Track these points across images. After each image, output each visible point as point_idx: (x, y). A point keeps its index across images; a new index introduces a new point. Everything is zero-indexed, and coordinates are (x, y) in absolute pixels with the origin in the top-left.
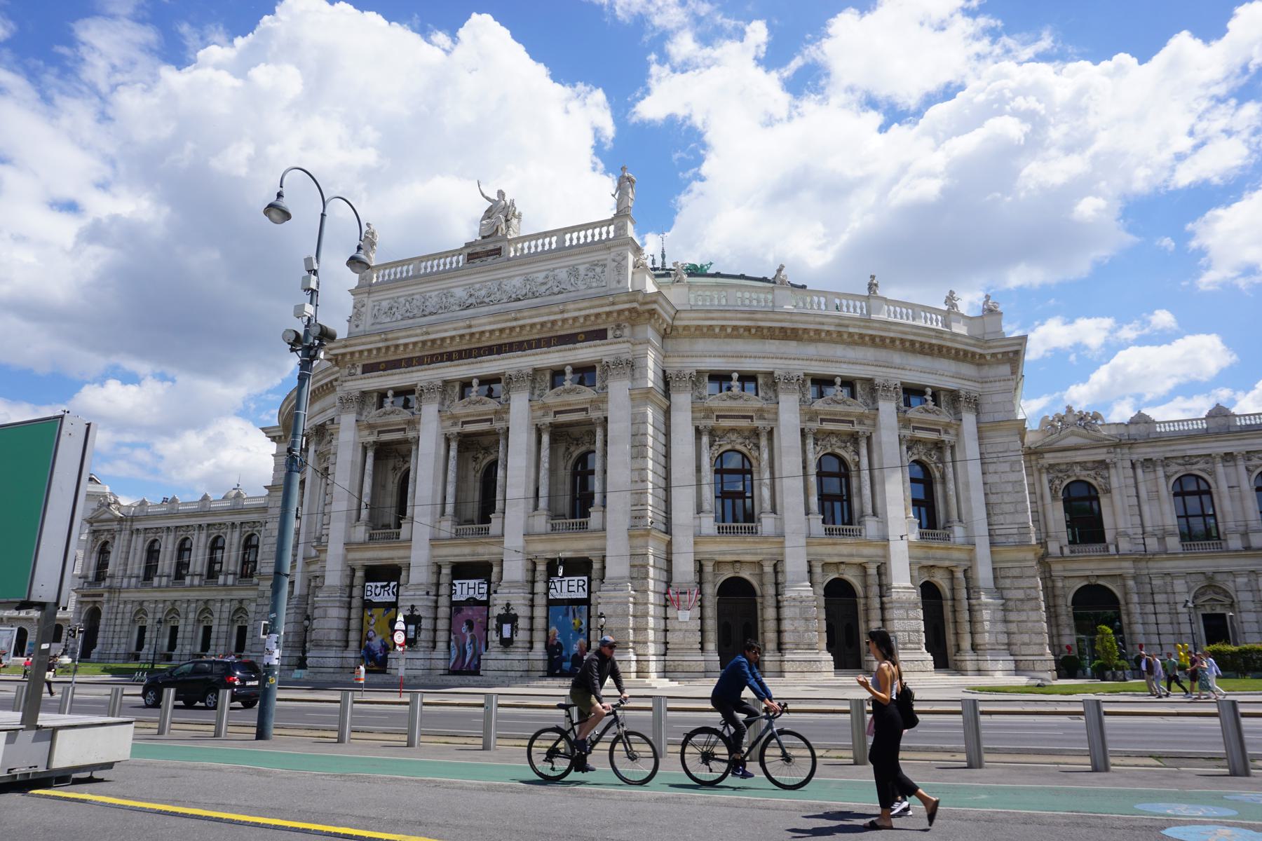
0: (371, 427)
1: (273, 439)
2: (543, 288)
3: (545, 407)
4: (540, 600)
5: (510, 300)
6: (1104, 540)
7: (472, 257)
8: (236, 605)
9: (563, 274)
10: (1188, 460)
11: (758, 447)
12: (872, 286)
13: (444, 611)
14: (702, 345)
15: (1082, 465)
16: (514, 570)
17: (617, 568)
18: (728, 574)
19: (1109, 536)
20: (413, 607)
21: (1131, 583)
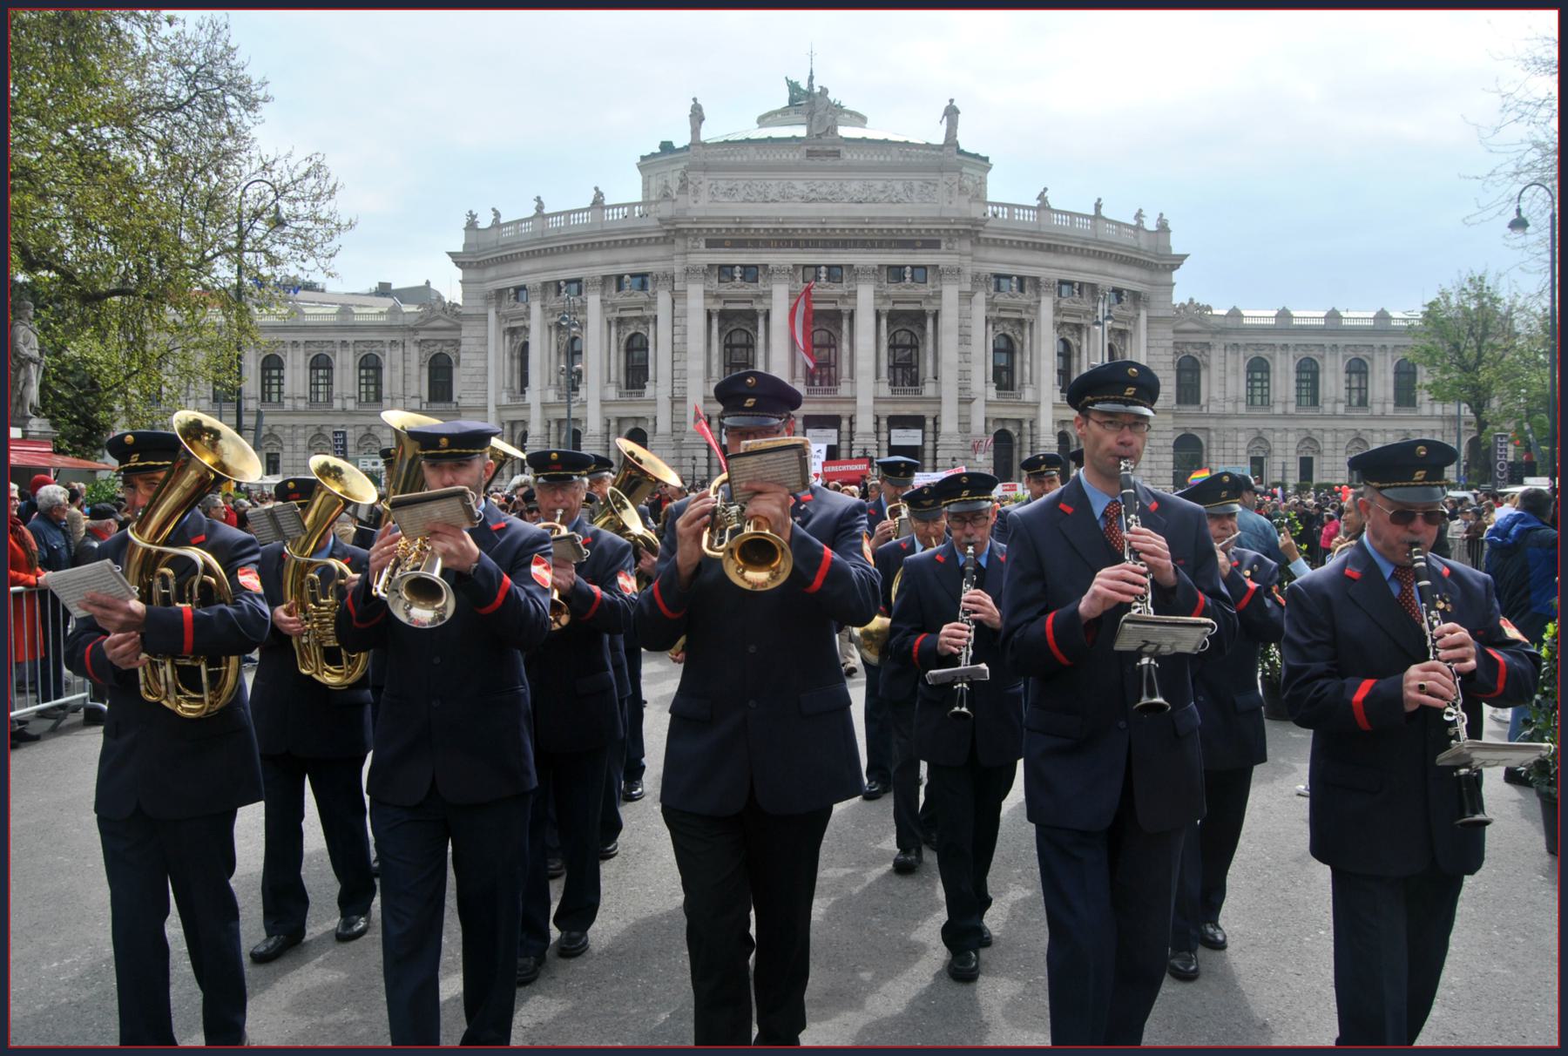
0: (718, 297)
1: (459, 264)
2: (882, 196)
3: (888, 297)
4: (885, 446)
5: (851, 201)
6: (1198, 402)
7: (810, 154)
8: (363, 431)
9: (899, 187)
10: (1258, 346)
11: (1022, 334)
12: (1098, 206)
14: (994, 254)
15: (1193, 344)
16: (865, 423)
17: (949, 425)
18: (999, 427)
19: (1203, 401)
21: (1213, 434)
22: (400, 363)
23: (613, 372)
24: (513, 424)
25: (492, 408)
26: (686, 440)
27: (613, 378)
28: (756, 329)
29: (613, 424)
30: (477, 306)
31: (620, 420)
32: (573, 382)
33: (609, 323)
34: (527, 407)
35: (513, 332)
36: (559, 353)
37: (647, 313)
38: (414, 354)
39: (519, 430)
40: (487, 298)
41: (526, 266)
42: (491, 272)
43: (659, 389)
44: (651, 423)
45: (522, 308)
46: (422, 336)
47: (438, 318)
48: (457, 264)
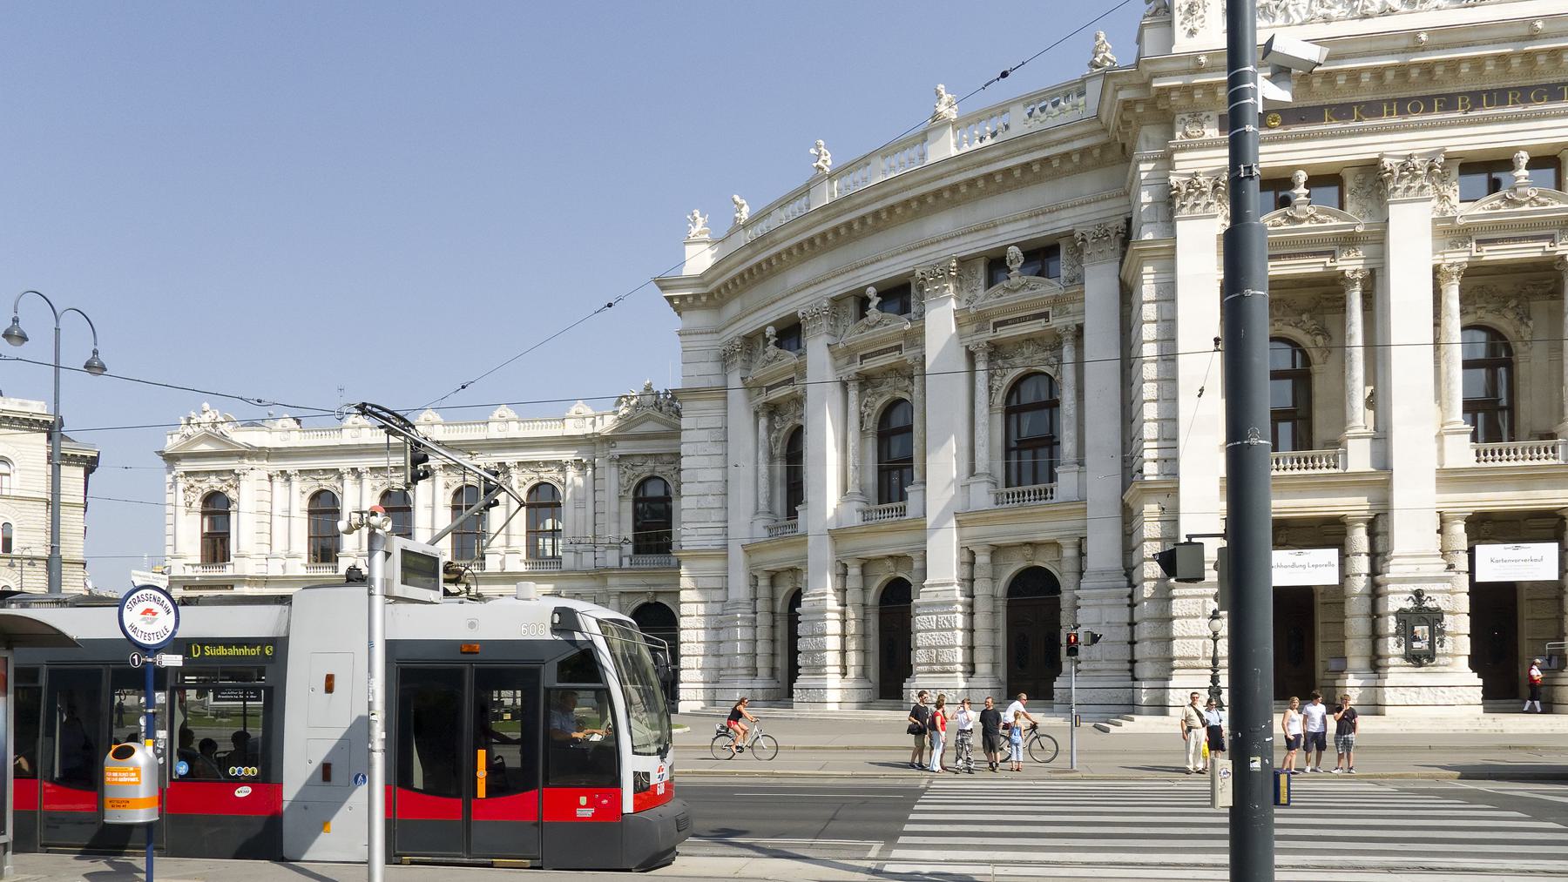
24: (774, 577)
25: (737, 555)
27: (981, 466)
30: (706, 373)
33: (971, 356)
35: (773, 410)
37: (1056, 323)
39: (783, 591)
40: (725, 359)
41: (797, 276)
42: (734, 308)
43: (1086, 481)
45: (790, 358)
46: (622, 448)
47: (648, 418)
48: (670, 299)
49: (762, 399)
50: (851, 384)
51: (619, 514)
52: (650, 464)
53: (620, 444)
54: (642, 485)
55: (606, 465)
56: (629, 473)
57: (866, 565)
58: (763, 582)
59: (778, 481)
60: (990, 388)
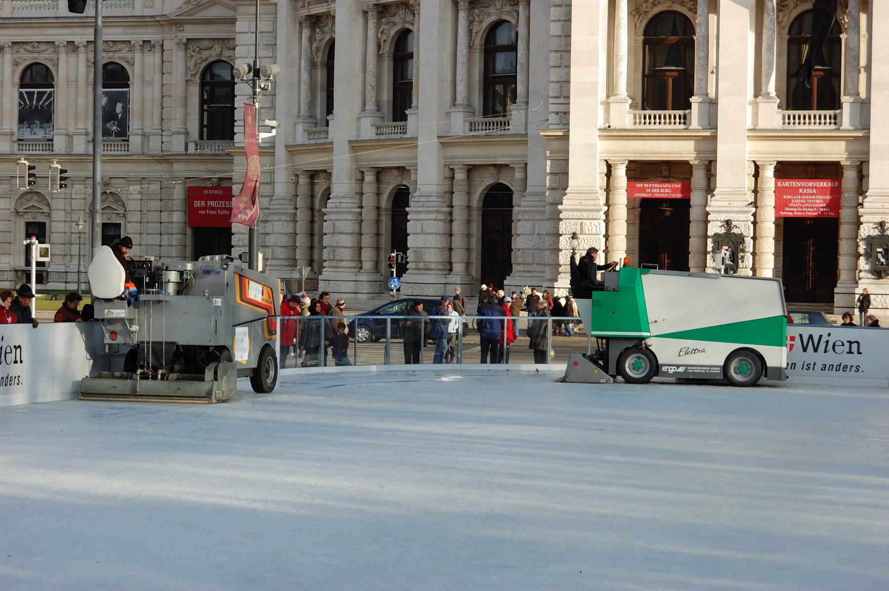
13: (769, 229)
20: (728, 223)
22: (157, 76)
23: (461, 88)
24: (313, 175)
25: (281, 152)
26: (568, 202)
27: (460, 100)
28: (694, 10)
29: (460, 176)
31: (471, 169)
32: (402, 99)
34: (328, 148)
36: (379, 57)
38: (177, 59)
44: (518, 175)
46: (191, 31)
49: (304, 12)
50: (370, 14)
51: (186, 98)
52: (217, 48)
53: (188, 27)
54: (209, 67)
55: (174, 47)
56: (196, 57)
57: (380, 172)
58: (303, 180)
59: (319, 87)
60: (470, 31)
